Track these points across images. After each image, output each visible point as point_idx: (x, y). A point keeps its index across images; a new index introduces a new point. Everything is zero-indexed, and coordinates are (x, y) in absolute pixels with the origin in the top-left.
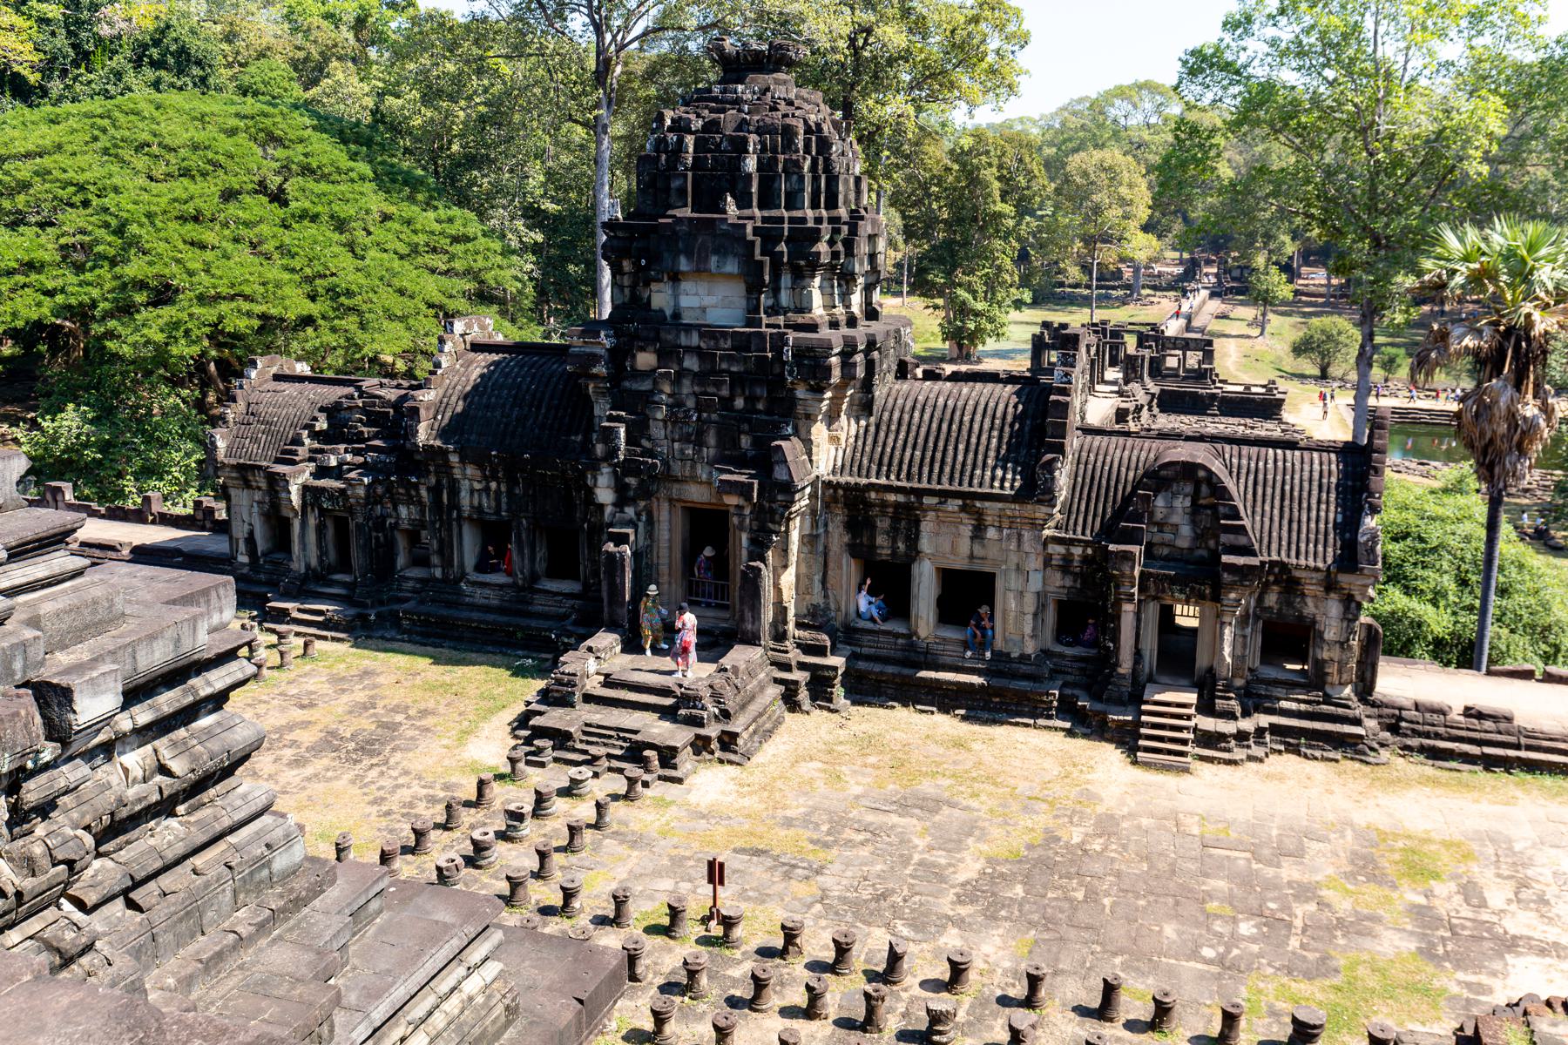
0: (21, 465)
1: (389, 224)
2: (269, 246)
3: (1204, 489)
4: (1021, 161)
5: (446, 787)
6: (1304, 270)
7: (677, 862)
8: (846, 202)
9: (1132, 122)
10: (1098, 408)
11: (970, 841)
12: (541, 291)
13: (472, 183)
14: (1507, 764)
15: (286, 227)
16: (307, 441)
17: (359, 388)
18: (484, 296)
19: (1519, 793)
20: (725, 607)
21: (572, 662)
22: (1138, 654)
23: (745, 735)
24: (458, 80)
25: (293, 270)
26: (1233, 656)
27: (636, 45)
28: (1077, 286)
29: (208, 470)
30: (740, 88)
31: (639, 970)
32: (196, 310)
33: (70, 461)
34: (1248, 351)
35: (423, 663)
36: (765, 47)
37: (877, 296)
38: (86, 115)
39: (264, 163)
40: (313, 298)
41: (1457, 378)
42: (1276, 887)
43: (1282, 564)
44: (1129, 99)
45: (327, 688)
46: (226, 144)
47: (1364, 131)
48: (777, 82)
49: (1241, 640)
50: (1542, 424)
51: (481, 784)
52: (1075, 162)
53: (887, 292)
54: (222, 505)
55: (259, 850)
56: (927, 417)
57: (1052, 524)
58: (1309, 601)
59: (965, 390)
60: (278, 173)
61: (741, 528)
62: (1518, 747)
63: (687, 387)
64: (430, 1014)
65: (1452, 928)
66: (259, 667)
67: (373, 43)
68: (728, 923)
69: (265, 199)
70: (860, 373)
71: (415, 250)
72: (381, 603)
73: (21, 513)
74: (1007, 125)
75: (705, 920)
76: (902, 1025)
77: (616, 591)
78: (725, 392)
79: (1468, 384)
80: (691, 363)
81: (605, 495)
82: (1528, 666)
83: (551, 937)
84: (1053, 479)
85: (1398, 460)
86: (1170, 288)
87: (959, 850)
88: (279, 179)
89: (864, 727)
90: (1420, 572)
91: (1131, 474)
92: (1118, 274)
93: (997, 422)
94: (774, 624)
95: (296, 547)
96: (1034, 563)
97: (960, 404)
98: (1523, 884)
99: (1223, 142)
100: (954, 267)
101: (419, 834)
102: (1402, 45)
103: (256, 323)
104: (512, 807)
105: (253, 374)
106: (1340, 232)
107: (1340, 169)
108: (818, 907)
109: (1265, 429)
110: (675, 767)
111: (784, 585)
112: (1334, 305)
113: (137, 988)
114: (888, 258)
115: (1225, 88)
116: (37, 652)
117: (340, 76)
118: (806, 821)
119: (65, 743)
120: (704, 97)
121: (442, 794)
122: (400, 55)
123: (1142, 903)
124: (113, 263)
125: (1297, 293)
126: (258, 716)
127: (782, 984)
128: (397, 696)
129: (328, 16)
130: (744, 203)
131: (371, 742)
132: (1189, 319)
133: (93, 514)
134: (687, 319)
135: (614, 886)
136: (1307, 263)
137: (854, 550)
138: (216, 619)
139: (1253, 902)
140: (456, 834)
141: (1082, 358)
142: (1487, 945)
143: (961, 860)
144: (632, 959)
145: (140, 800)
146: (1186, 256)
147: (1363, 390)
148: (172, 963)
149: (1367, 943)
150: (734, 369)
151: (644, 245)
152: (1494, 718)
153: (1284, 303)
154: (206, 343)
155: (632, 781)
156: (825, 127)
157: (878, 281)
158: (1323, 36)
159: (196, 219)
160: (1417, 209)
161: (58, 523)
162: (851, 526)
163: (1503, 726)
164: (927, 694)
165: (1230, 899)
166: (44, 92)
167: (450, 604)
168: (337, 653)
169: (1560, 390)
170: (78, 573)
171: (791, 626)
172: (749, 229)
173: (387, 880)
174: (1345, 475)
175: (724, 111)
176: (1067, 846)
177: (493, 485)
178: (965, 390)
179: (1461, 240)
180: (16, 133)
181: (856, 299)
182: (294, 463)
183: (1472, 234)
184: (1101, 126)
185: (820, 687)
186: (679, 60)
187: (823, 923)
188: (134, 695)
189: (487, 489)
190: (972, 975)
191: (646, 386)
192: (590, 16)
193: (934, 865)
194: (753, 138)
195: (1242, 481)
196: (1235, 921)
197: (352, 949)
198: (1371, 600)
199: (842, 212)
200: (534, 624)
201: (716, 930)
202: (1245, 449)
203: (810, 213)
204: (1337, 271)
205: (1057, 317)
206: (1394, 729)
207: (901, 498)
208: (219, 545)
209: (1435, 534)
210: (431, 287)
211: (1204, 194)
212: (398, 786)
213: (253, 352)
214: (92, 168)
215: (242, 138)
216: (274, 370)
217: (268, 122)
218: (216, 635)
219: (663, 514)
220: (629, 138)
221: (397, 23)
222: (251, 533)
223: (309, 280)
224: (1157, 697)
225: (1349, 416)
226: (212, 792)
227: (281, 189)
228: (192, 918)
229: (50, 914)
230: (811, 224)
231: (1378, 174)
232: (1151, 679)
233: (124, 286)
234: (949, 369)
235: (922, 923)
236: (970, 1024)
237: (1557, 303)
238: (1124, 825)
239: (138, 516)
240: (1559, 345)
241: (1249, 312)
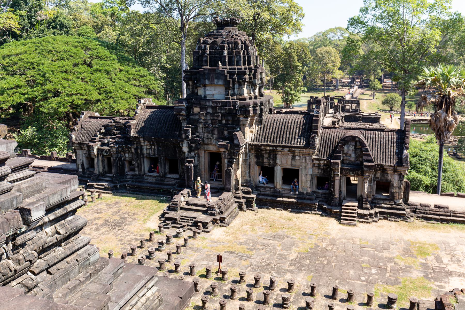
0: (15, 144)
1: (122, 72)
2: (87, 79)
3: (358, 144)
4: (303, 50)
5: (141, 236)
6: (385, 80)
7: (208, 256)
8: (253, 63)
9: (335, 39)
10: (327, 121)
11: (293, 247)
12: (166, 91)
13: (146, 60)
14: (447, 221)
15: (92, 74)
16: (99, 136)
17: (114, 120)
18: (150, 92)
19: (451, 230)
20: (221, 181)
21: (177, 198)
22: (340, 192)
23: (227, 218)
24: (141, 31)
25: (94, 86)
26: (368, 192)
27: (192, 19)
28: (320, 86)
29: (70, 145)
30: (222, 31)
31: (198, 288)
32: (66, 98)
33: (30, 143)
34: (369, 104)
35: (133, 199)
36: (229, 19)
37: (263, 90)
38: (34, 43)
39: (85, 55)
40: (100, 94)
41: (429, 110)
42: (382, 259)
43: (381, 165)
44: (333, 32)
45: (105, 208)
46: (74, 50)
47: (400, 40)
48: (233, 29)
49: (370, 187)
50: (454, 123)
51: (151, 234)
52: (319, 50)
53: (266, 89)
54: (74, 155)
55: (86, 256)
56: (278, 124)
57: (315, 154)
58: (389, 175)
59: (289, 117)
60: (89, 58)
61: (225, 158)
62: (450, 216)
63: (209, 117)
64: (137, 303)
65: (433, 269)
66: (85, 202)
67: (116, 20)
68: (223, 273)
69: (86, 66)
70: (258, 112)
71: (129, 80)
72: (121, 182)
73: (15, 158)
74: (299, 40)
75: (217, 273)
76: (275, 302)
77: (189, 177)
78: (220, 119)
79: (433, 112)
80: (210, 110)
81: (185, 149)
82: (452, 193)
83: (172, 279)
84: (315, 142)
85: (413, 134)
86: (347, 86)
87: (290, 250)
88: (90, 60)
89: (262, 215)
90: (420, 166)
91: (337, 140)
92: (332, 82)
93: (298, 125)
94: (235, 186)
95: (96, 166)
96: (310, 166)
97: (287, 120)
98: (453, 256)
99: (361, 44)
100: (285, 81)
101: (133, 250)
102: (411, 15)
103: (84, 102)
104: (160, 241)
105: (83, 116)
106: (395, 69)
107: (394, 51)
108: (250, 268)
109: (375, 126)
110: (207, 228)
111: (238, 173)
112: (394, 90)
113: (50, 297)
114: (266, 79)
115: (361, 29)
116: (20, 199)
117: (107, 30)
118: (246, 243)
119: (29, 225)
120: (212, 34)
121: (139, 238)
122: (124, 24)
123: (343, 264)
124: (42, 85)
125: (383, 86)
126: (85, 216)
127: (240, 291)
128: (125, 209)
129: (103, 13)
130: (224, 64)
131: (118, 223)
132: (352, 95)
133: (36, 158)
135: (190, 263)
136: (386, 78)
137: (258, 163)
138: (73, 188)
139: (376, 263)
140: (144, 249)
141: (322, 106)
142: (443, 274)
143: (291, 253)
144: (196, 285)
145: (51, 242)
146: (351, 77)
147: (403, 114)
148: (61, 290)
149: (409, 274)
150: (222, 112)
151: (195, 77)
152: (443, 208)
153: (379, 89)
154: (69, 108)
155: (195, 233)
156: (247, 42)
157: (263, 86)
158: (388, 13)
159: (66, 72)
160: (416, 62)
161: (26, 161)
162: (257, 157)
163: (446, 210)
164: (280, 205)
165: (369, 263)
166: (21, 37)
167: (141, 182)
168: (108, 197)
169: (459, 113)
170: (32, 176)
171: (240, 186)
172: (226, 72)
173: (123, 264)
174: (398, 139)
175: (218, 38)
176: (321, 248)
177: (153, 147)
178: (289, 117)
179: (429, 71)
180: (13, 48)
181: (257, 91)
182: (95, 142)
183: (432, 69)
184: (326, 40)
185: (249, 204)
186: (205, 24)
187: (251, 273)
188: (49, 211)
189: (151, 148)
190: (295, 287)
191: (197, 117)
192: (179, 11)
193: (283, 255)
194: (226, 45)
195: (369, 141)
196: (370, 269)
197: (114, 284)
198: (407, 174)
199: (252, 66)
200: (165, 187)
201: (220, 275)
202: (369, 132)
203: (243, 67)
204: (394, 80)
205: (315, 95)
206: (414, 212)
207: (271, 148)
208: (73, 166)
209: (424, 155)
210: (134, 90)
211: (356, 59)
212: (126, 236)
213: (83, 110)
214: (35, 58)
215: (79, 48)
216: (89, 115)
217: (86, 44)
218: (72, 193)
219: (202, 154)
220: (191, 46)
221: (123, 15)
222: (83, 163)
223: (99, 89)
224: (346, 204)
225: (399, 122)
226: (72, 239)
227: (90, 63)
228: (66, 276)
229: (25, 276)
230: (243, 70)
231: (405, 52)
232: (344, 199)
233: (45, 92)
234: (284, 110)
235: (280, 272)
236: (294, 301)
237: (457, 88)
238: (338, 242)
239: (50, 159)
240: (458, 100)
241: (370, 92)
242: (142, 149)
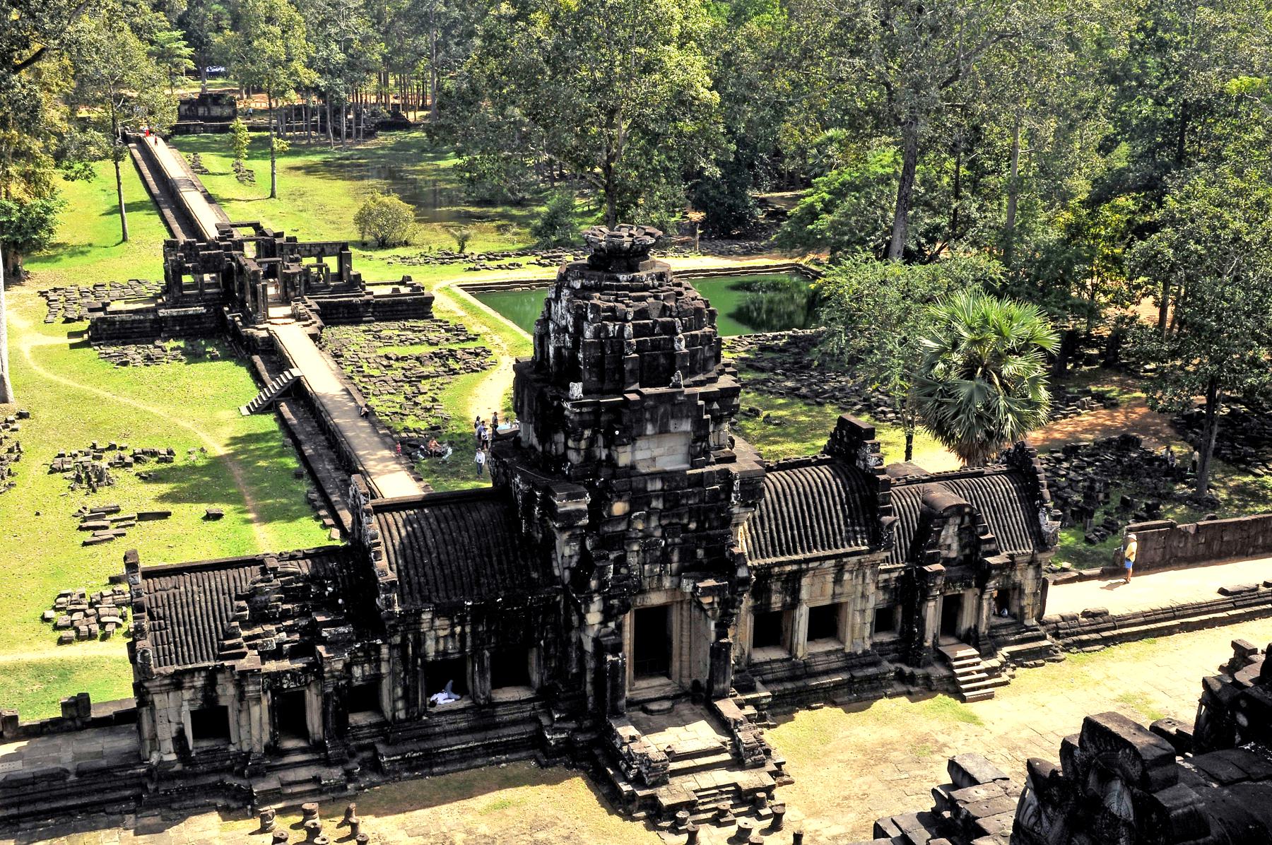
62: (1114, 628)
78: (685, 521)
134: (643, 469)
191: (622, 527)
207: (795, 567)
242: (419, 642)
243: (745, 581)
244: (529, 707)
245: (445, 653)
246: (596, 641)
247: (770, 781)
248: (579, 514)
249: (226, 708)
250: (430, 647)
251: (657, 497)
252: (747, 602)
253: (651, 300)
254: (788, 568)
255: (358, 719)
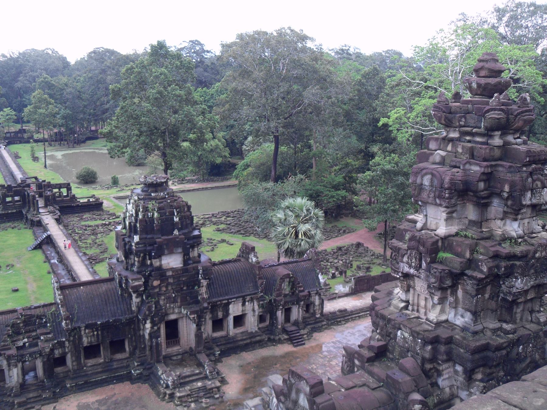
191: (157, 290)
207: (226, 301)
243: (207, 308)
244: (126, 361)
245: (91, 342)
246: (150, 334)
247: (218, 384)
248: (140, 286)
249: (3, 370)
250: (85, 340)
251: (171, 278)
252: (208, 316)
253: (165, 203)
254: (224, 302)
255: (59, 370)
